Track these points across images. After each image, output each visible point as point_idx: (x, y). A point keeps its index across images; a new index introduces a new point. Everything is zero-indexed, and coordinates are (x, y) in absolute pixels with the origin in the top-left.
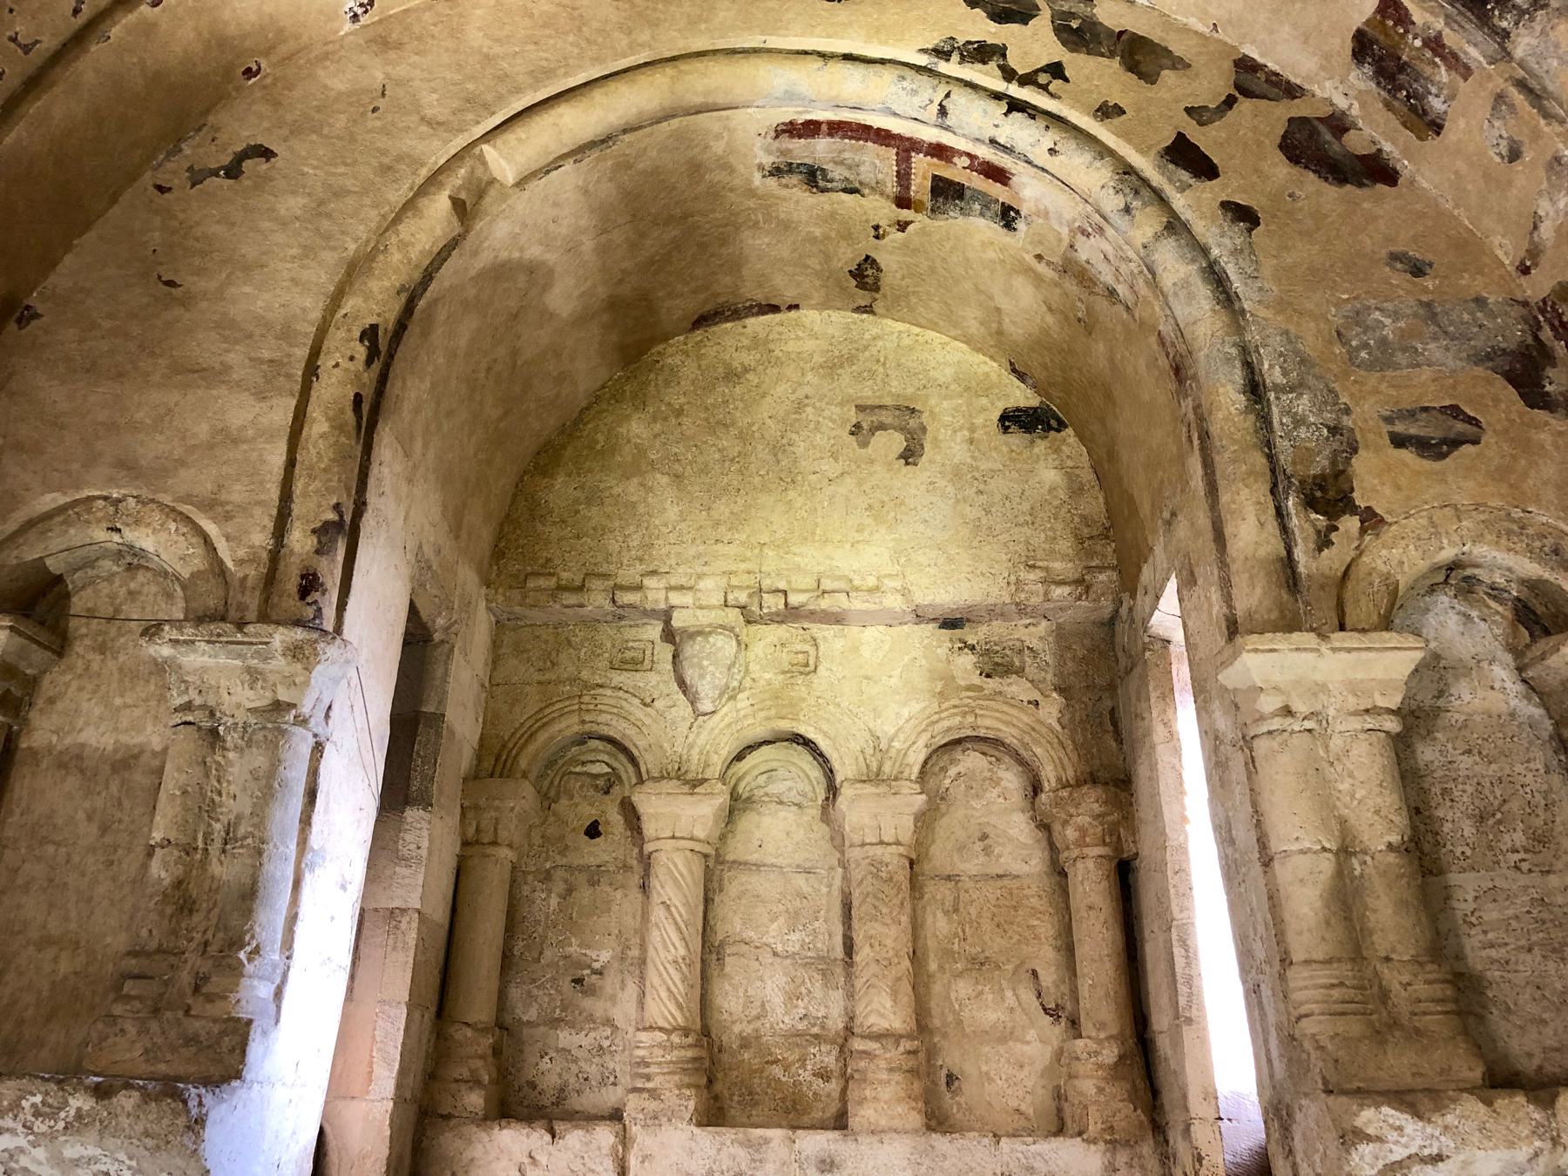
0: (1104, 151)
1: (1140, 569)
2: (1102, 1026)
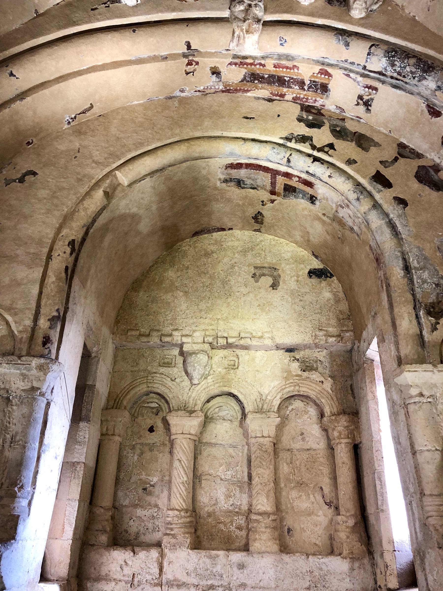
0: (349, 177)
1: (362, 332)
2: (348, 511)
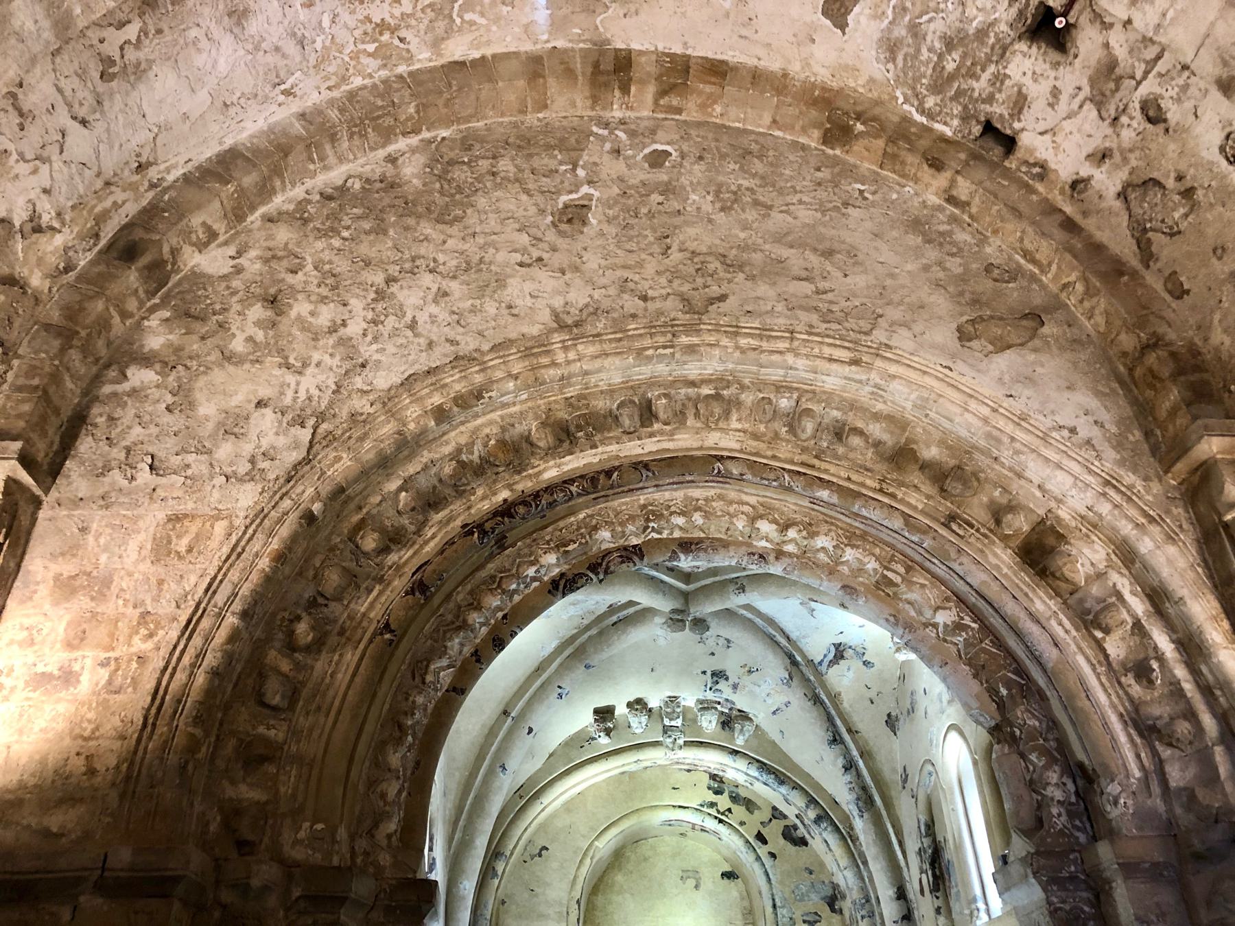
0: (742, 836)
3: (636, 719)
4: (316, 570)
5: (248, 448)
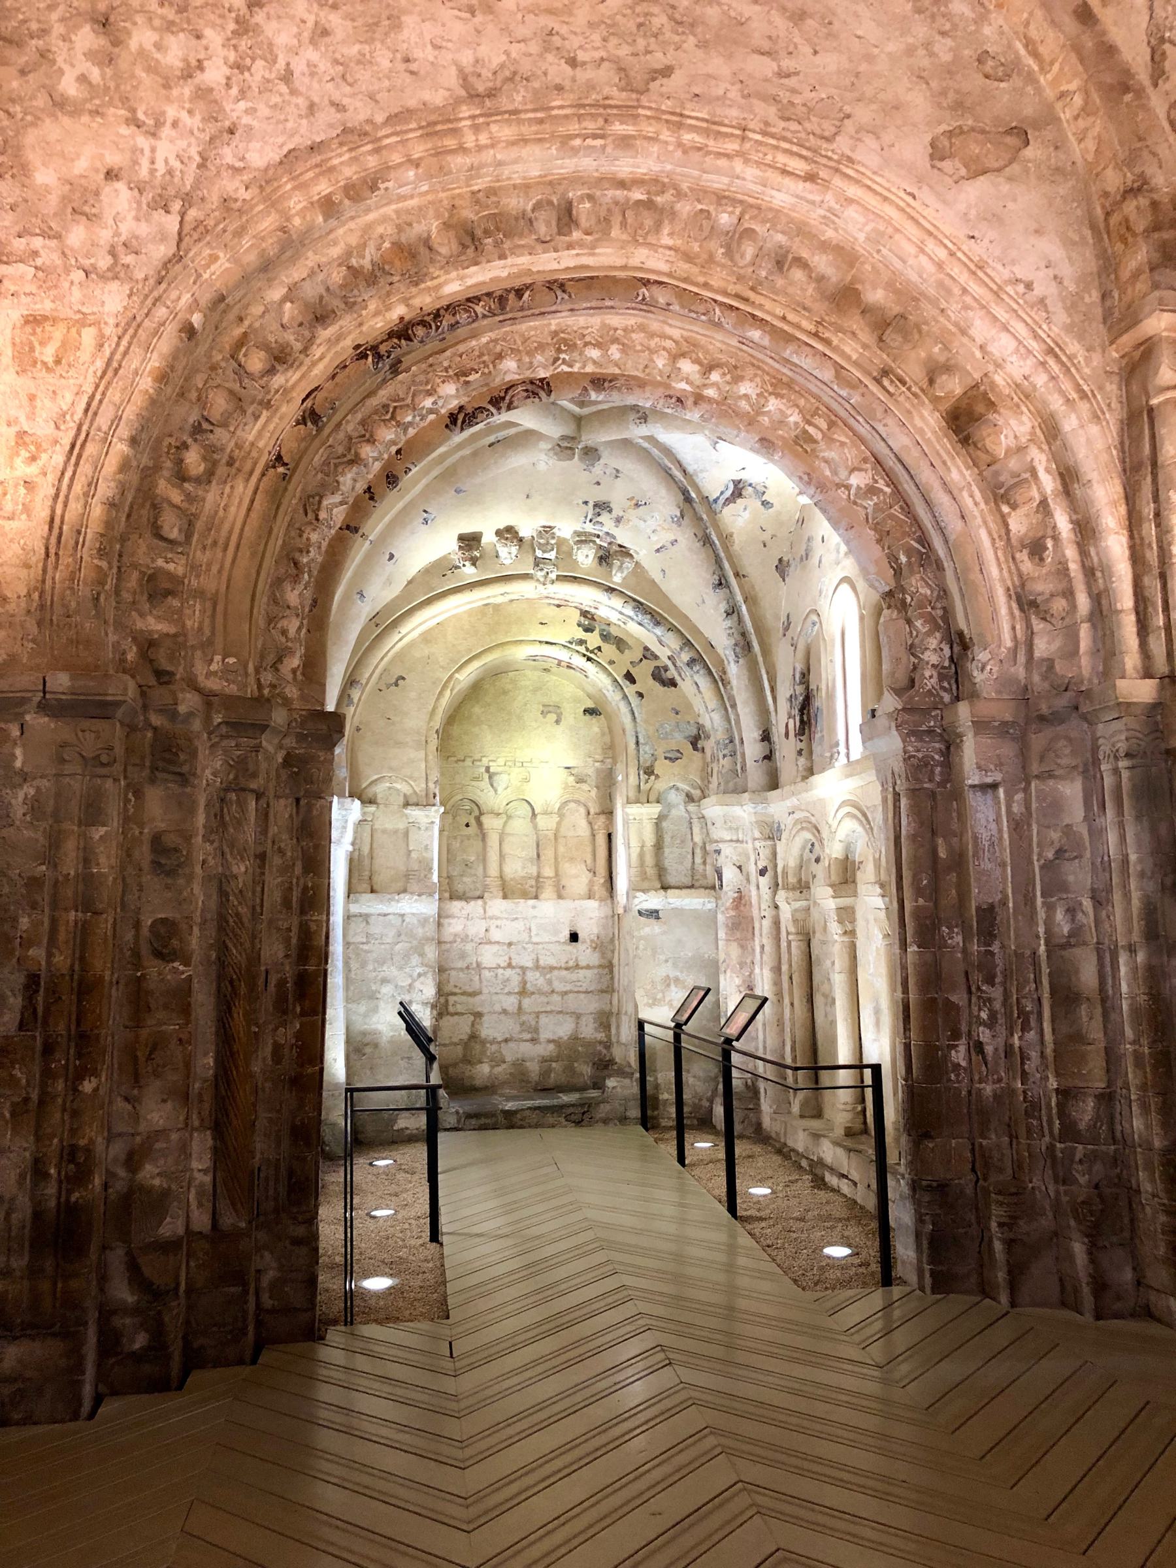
0: (610, 674)
3: (506, 550)
4: (199, 390)
5: (105, 235)
